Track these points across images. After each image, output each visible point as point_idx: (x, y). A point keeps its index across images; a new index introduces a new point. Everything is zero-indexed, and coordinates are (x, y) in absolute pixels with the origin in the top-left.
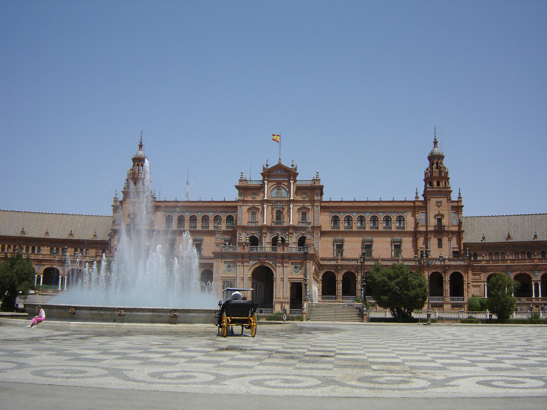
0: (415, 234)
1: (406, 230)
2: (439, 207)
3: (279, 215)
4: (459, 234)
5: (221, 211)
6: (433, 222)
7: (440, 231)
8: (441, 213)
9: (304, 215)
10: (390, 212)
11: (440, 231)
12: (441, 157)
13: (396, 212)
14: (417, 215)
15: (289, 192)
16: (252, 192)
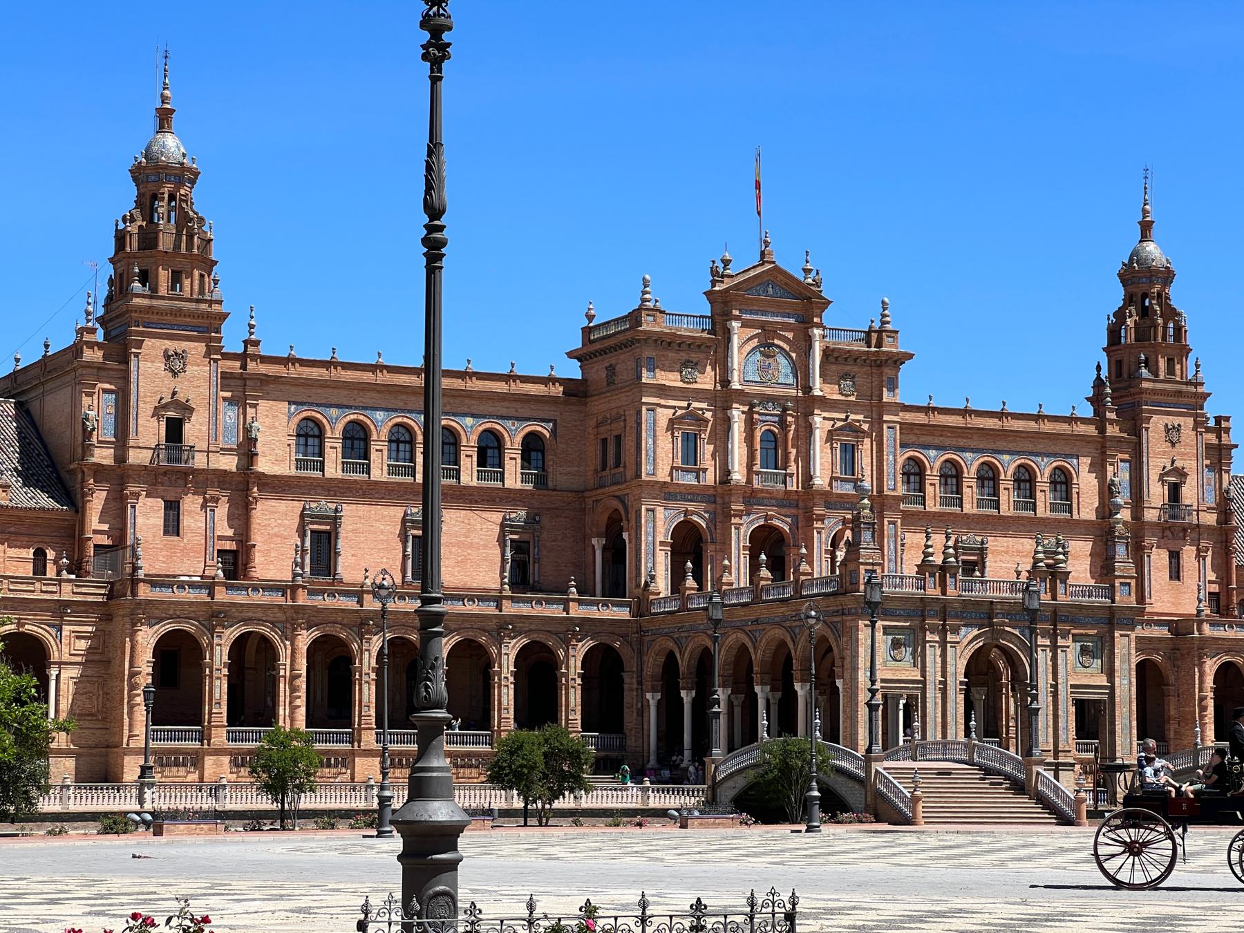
0: (1103, 533)
1: (1075, 516)
2: (1173, 445)
3: (773, 449)
4: (1223, 535)
5: (504, 412)
6: (1156, 493)
7: (1175, 529)
8: (1178, 464)
9: (849, 452)
10: (1031, 453)
11: (1175, 529)
12: (1167, 276)
13: (1049, 455)
14: (1110, 469)
15: (801, 370)
16: (684, 356)
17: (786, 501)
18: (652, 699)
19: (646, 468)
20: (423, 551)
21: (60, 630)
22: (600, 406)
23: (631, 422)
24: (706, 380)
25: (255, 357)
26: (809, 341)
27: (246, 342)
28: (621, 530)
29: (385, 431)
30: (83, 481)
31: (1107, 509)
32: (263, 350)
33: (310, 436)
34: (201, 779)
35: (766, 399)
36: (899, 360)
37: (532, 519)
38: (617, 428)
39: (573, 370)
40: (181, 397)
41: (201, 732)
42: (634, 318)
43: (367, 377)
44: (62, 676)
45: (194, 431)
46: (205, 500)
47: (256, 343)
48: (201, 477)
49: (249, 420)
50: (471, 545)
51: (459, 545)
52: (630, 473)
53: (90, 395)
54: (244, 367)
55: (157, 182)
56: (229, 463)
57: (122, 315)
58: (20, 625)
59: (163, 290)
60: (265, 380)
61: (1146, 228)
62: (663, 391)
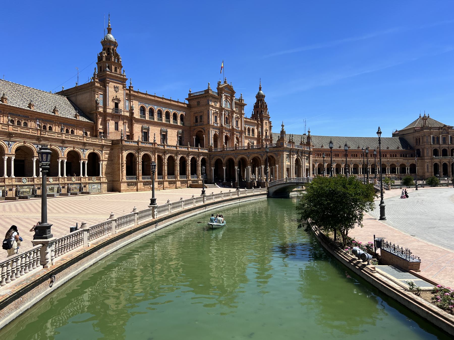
9: (237, 122)
12: (264, 96)
17: (229, 131)
18: (213, 168)
19: (210, 122)
20: (164, 137)
21: (102, 152)
22: (195, 110)
23: (206, 112)
24: (218, 105)
25: (132, 90)
26: (232, 100)
27: (130, 87)
28: (203, 135)
29: (157, 111)
30: (96, 116)
31: (259, 136)
32: (134, 89)
33: (143, 110)
34: (137, 188)
35: (227, 110)
36: (245, 105)
37: (183, 131)
38: (200, 114)
39: (187, 102)
40: (118, 97)
41: (136, 177)
42: (207, 91)
43: (153, 98)
44: (103, 164)
45: (121, 106)
46: (124, 123)
47: (132, 87)
48: (123, 117)
49: (131, 105)
50: (172, 137)
51: (170, 136)
52: (206, 122)
53: (97, 94)
54: (130, 92)
55: (108, 45)
56: (128, 114)
57: (104, 76)
58: (94, 150)
59: (113, 71)
60: (134, 96)
61: (260, 89)
62: (212, 106)
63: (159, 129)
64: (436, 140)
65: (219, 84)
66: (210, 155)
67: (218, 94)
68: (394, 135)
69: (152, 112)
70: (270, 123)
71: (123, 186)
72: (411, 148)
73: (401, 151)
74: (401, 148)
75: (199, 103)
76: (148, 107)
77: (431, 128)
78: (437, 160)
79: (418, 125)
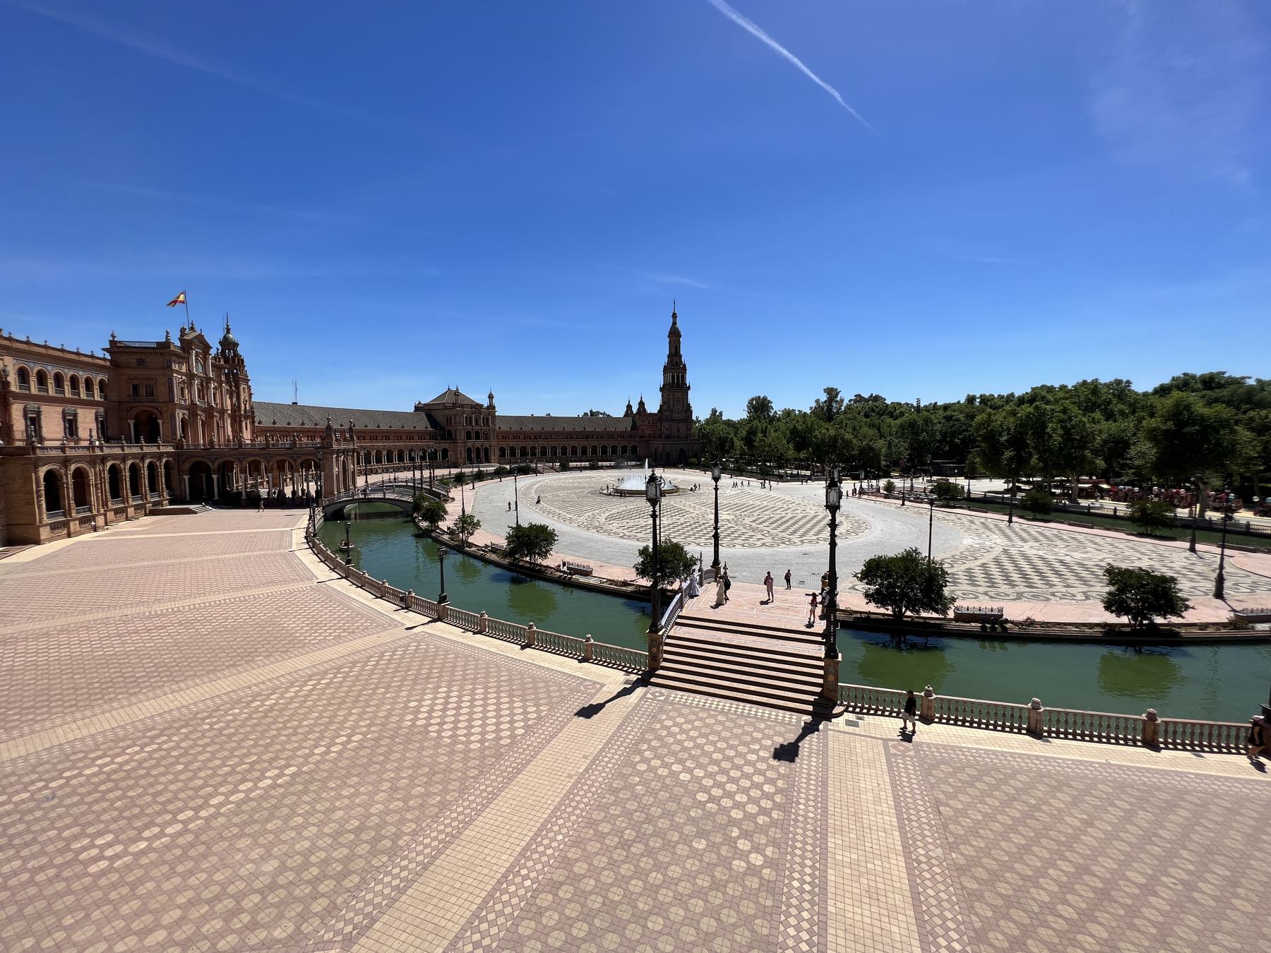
3: (203, 392)
12: (236, 345)
18: (186, 477)
33: (23, 375)
37: (106, 411)
39: (108, 356)
42: (165, 345)
63: (60, 409)
64: (469, 420)
65: (183, 330)
66: (178, 456)
67: (182, 348)
68: (417, 408)
69: (42, 378)
70: (249, 387)
71: (44, 533)
72: (442, 429)
73: (429, 433)
74: (430, 428)
75: (141, 363)
76: (34, 368)
77: (462, 406)
78: (470, 444)
79: (449, 400)
